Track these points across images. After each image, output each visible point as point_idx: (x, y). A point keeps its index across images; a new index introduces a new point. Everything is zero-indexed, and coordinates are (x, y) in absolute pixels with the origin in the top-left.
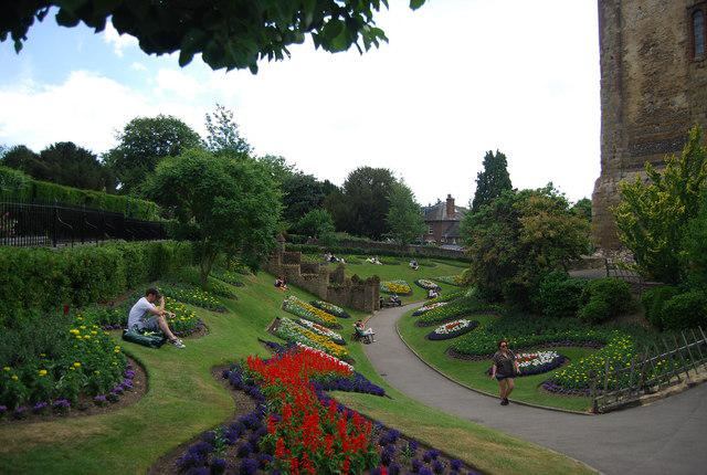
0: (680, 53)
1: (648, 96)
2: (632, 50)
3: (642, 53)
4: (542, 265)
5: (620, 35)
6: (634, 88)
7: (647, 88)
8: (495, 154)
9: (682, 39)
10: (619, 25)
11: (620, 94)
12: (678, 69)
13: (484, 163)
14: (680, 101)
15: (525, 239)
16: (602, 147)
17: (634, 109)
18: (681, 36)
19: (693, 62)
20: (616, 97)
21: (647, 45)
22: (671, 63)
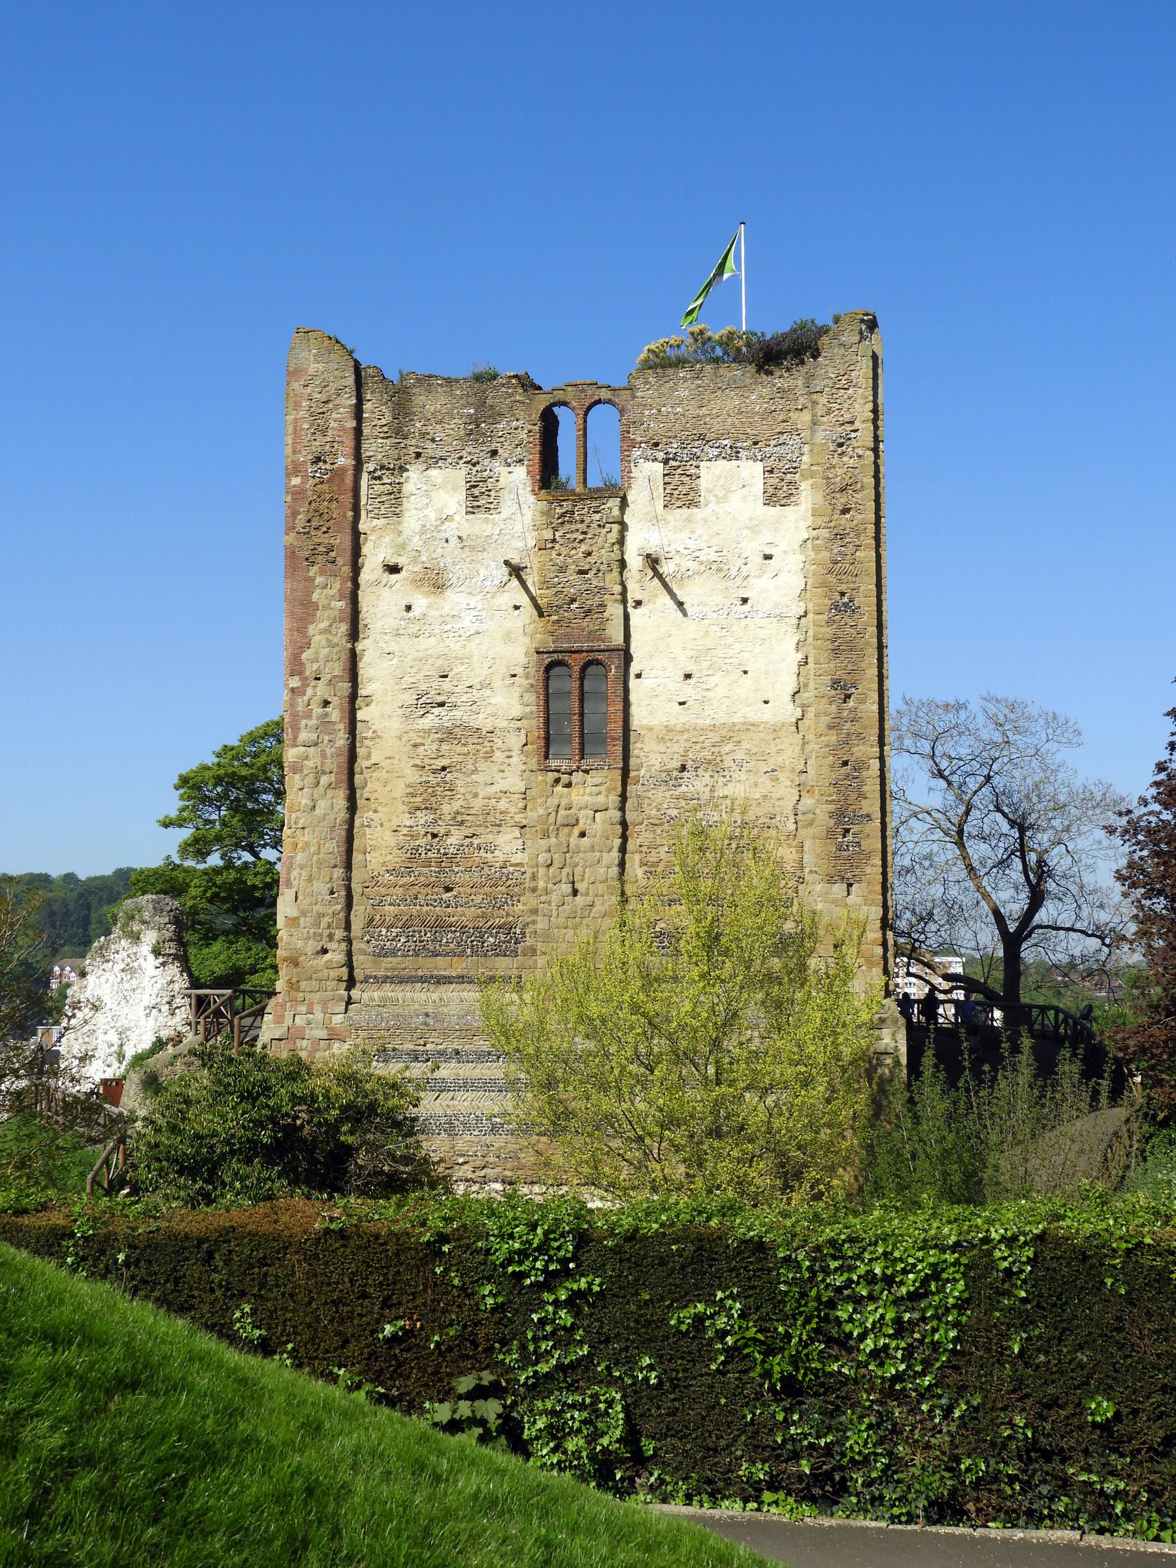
1: (423, 817)
7: (425, 799)
9: (517, 711)
14: (507, 846)
22: (489, 756)
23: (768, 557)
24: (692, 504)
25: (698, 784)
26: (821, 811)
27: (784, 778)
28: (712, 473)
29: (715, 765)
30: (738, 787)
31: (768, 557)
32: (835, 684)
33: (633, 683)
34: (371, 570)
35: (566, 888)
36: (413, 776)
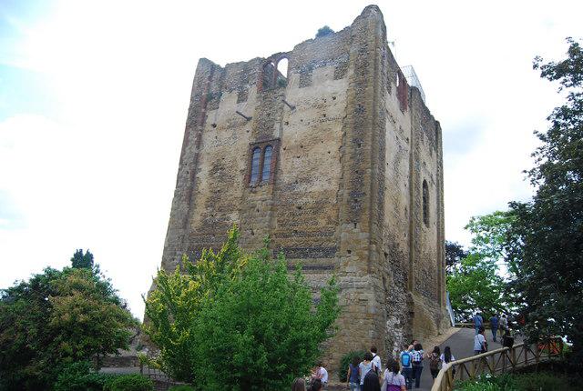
0: (240, 179)
1: (210, 209)
2: (205, 168)
3: (211, 173)
4: (66, 355)
5: (197, 155)
6: (201, 201)
7: (213, 200)
8: (84, 253)
9: (243, 168)
10: (198, 147)
11: (189, 204)
12: (236, 191)
13: (72, 260)
15: (54, 321)
16: (165, 249)
17: (197, 219)
18: (242, 165)
19: (248, 187)
20: (185, 205)
21: (217, 168)
22: (232, 186)
23: (334, 98)
24: (308, 85)
25: (301, 188)
26: (345, 193)
27: (333, 182)
28: (316, 73)
29: (307, 180)
30: (316, 187)
31: (334, 98)
32: (355, 141)
33: (282, 151)
34: (208, 127)
35: (249, 232)
36: (209, 195)
